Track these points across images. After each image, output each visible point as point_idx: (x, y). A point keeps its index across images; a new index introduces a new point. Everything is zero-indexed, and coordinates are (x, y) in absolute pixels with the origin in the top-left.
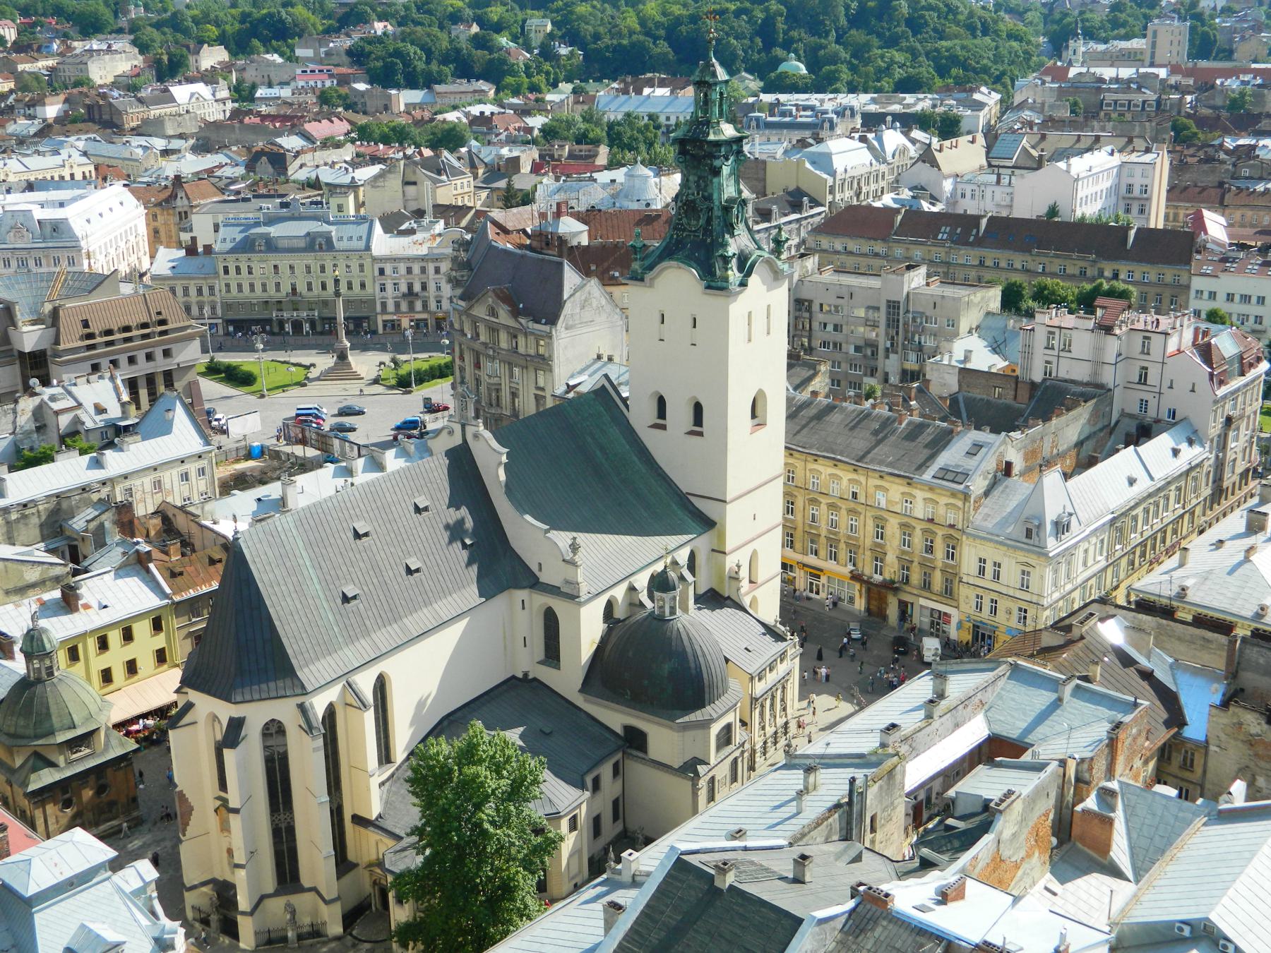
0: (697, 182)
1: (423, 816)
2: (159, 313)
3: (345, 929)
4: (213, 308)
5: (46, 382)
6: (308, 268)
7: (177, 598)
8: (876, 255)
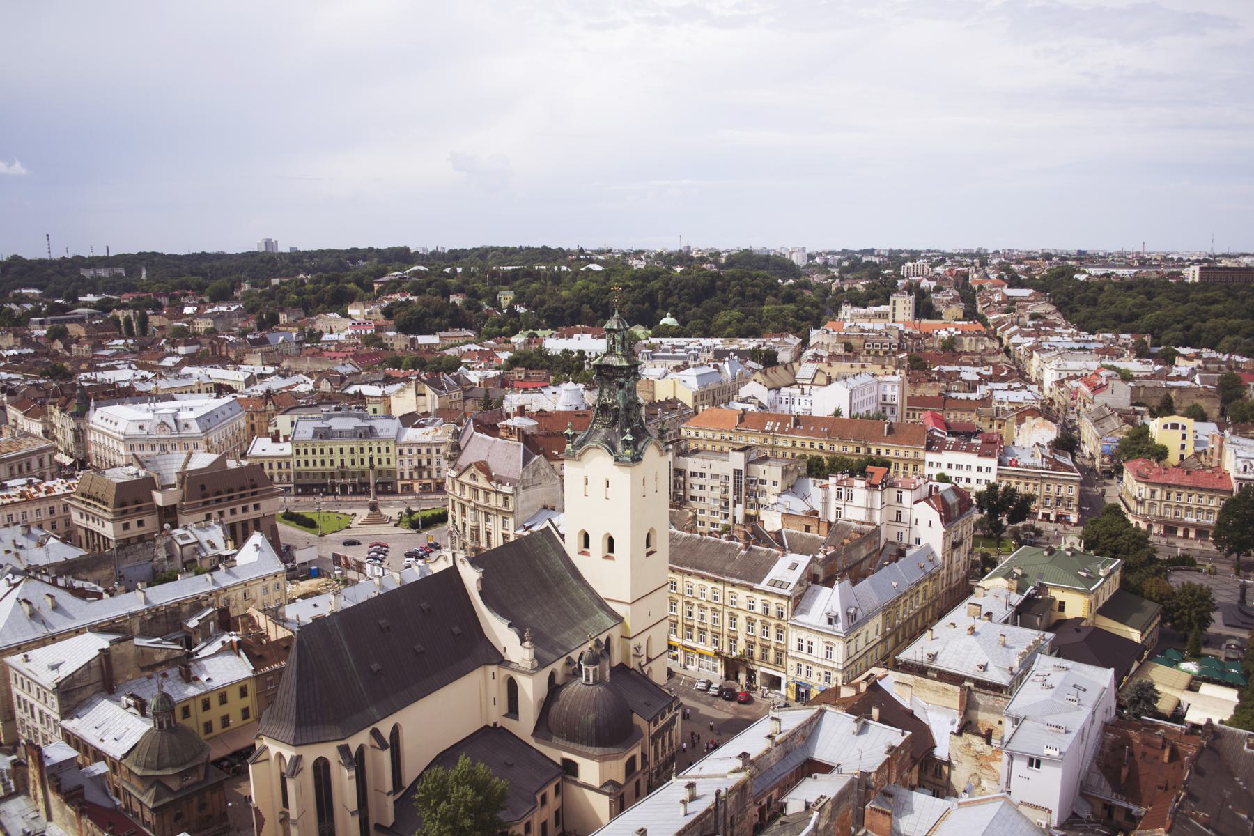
4: (289, 477)
5: (175, 526)
6: (352, 450)
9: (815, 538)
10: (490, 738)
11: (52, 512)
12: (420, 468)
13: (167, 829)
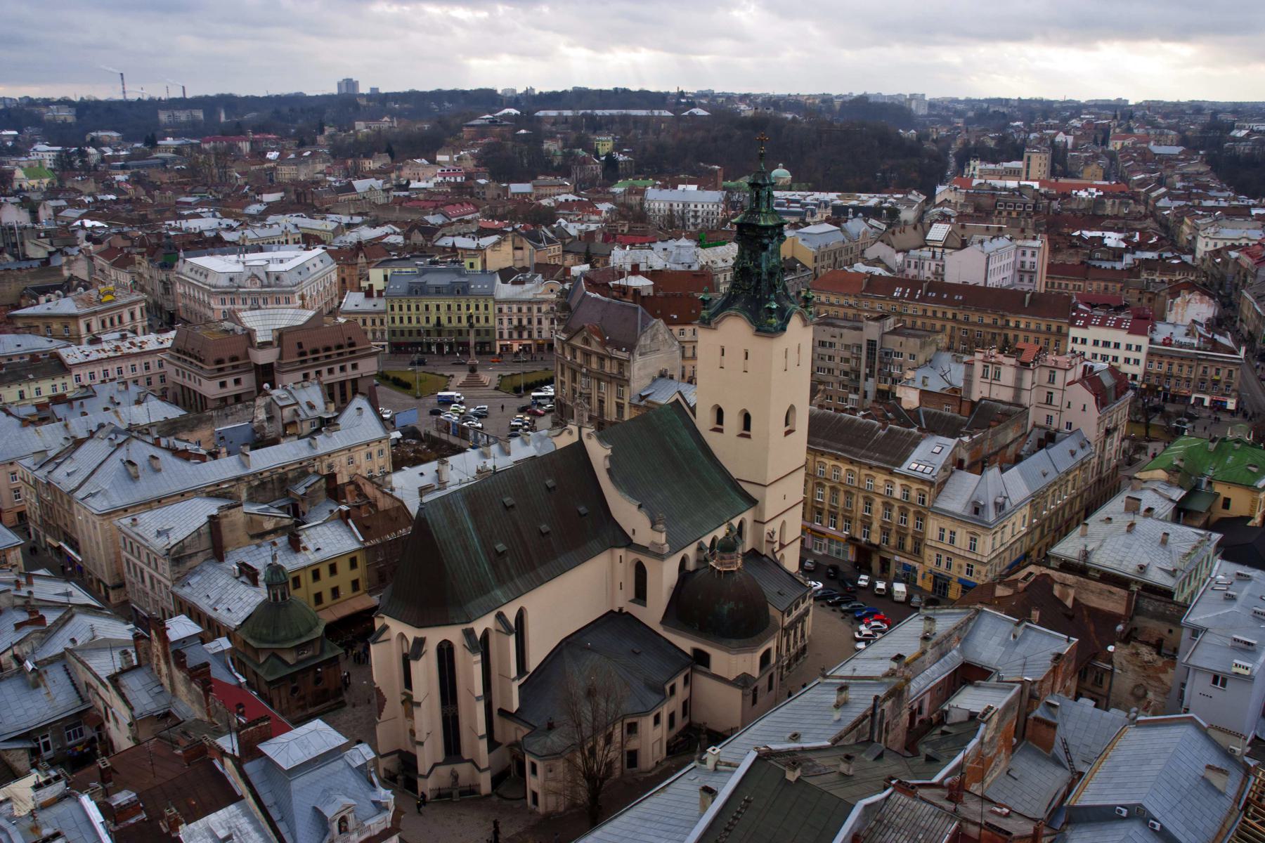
0: (750, 255)
3: (493, 788)
4: (383, 334)
5: (273, 387)
6: (449, 306)
7: (368, 544)
10: (615, 623)
11: (147, 368)
12: (520, 328)
13: (284, 701)
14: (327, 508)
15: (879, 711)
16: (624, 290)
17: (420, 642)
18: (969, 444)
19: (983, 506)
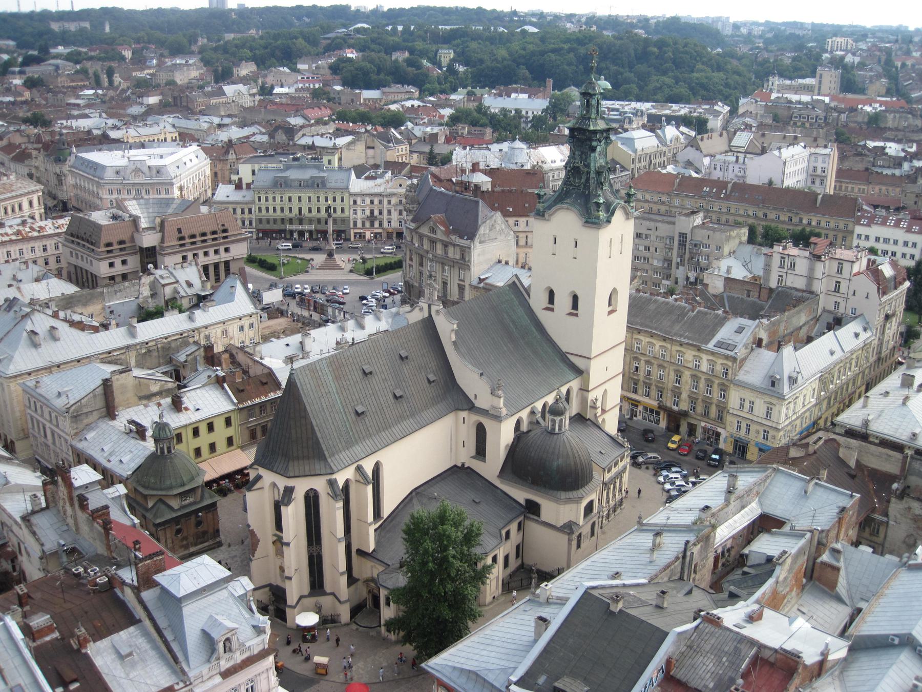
1: (408, 552)
2: (223, 225)
3: (352, 617)
5: (156, 267)
6: (310, 198)
7: (241, 406)
8: (663, 203)
9: (754, 303)
11: (45, 250)
13: (169, 541)
14: (205, 373)
15: (688, 554)
16: (465, 186)
17: (289, 491)
18: (768, 325)
19: (779, 380)
